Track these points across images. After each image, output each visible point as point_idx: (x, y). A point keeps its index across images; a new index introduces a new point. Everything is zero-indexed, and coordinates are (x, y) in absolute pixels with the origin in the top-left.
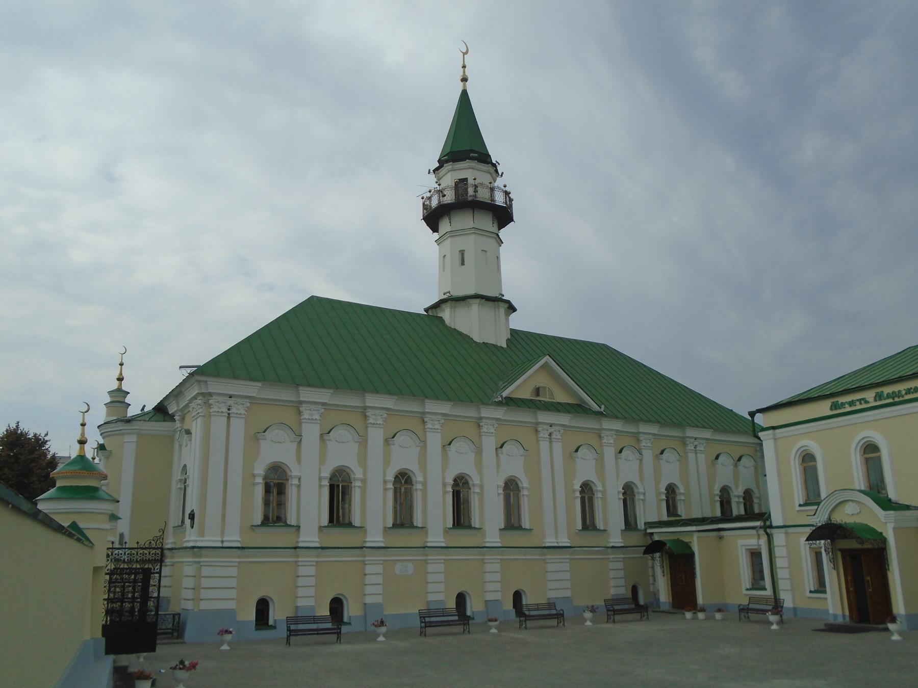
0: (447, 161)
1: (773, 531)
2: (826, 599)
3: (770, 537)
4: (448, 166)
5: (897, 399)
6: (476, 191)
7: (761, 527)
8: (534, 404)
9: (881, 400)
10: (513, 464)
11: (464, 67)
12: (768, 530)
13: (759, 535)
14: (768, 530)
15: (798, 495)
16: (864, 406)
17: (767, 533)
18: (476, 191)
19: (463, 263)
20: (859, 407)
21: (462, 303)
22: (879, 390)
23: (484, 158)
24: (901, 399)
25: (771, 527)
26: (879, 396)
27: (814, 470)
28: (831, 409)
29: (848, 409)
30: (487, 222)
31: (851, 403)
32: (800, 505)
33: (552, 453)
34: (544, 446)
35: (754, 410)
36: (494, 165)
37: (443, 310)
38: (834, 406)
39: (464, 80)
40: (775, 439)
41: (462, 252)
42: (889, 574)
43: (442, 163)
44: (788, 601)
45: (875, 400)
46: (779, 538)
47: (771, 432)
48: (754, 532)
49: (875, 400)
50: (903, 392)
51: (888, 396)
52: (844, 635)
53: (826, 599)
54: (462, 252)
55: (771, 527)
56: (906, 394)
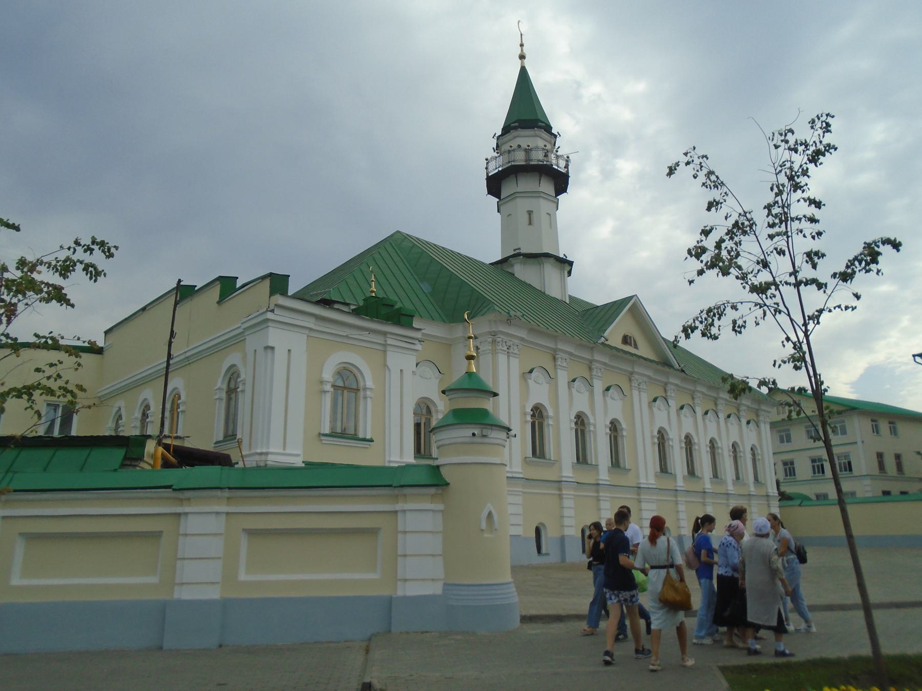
0: (515, 128)
4: (513, 133)
6: (546, 156)
8: (623, 355)
10: (615, 408)
11: (522, 45)
18: (546, 156)
19: (530, 223)
21: (533, 260)
23: (548, 128)
30: (547, 187)
33: (640, 399)
34: (635, 393)
36: (555, 136)
37: (512, 266)
39: (522, 57)
41: (530, 213)
43: (506, 130)
54: (530, 213)
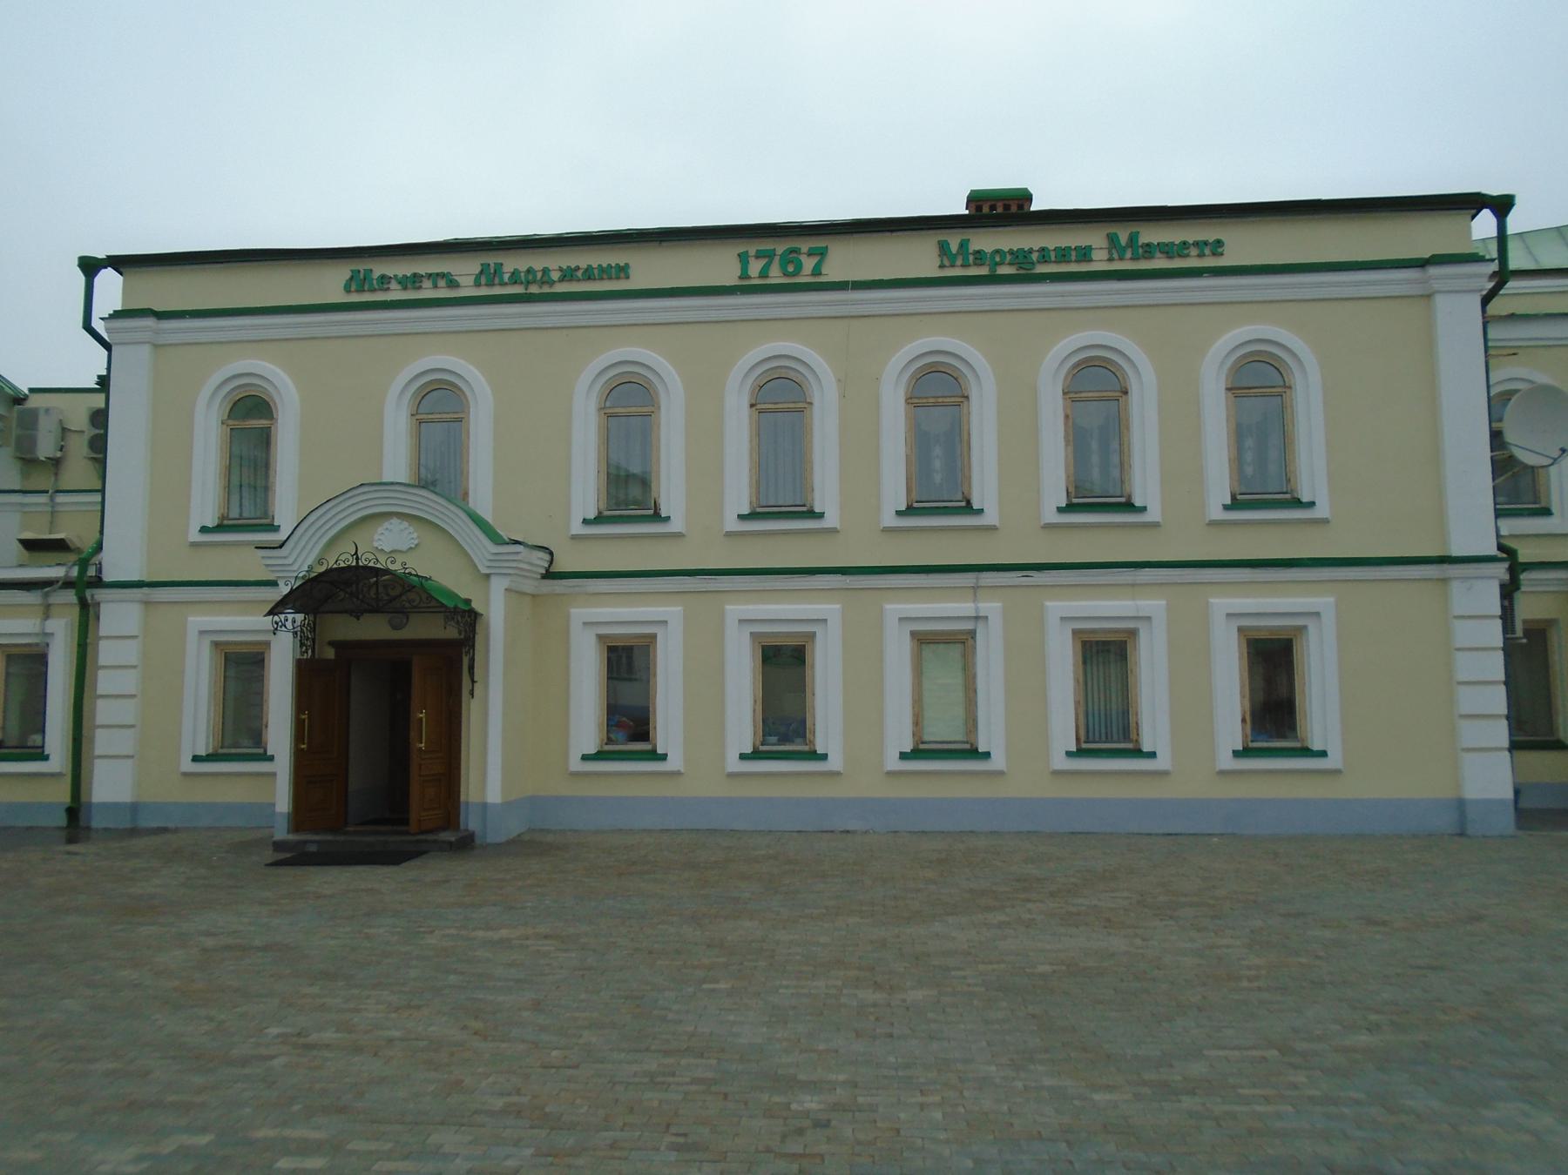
1: (100, 594)
2: (274, 775)
3: (87, 613)
5: (534, 289)
7: (68, 584)
9: (491, 284)
12: (88, 593)
13: (48, 607)
14: (88, 593)
15: (205, 504)
16: (443, 293)
17: (84, 605)
20: (427, 293)
22: (492, 259)
24: (546, 289)
25: (98, 583)
26: (489, 275)
27: (265, 439)
28: (348, 290)
29: (396, 294)
31: (415, 281)
32: (204, 530)
35: (101, 255)
38: (358, 282)
40: (156, 346)
42: (472, 711)
44: (110, 785)
45: (477, 284)
46: (118, 616)
47: (150, 322)
48: (32, 598)
49: (477, 284)
50: (555, 276)
51: (515, 279)
52: (311, 869)
53: (274, 775)
55: (98, 583)
56: (562, 280)
